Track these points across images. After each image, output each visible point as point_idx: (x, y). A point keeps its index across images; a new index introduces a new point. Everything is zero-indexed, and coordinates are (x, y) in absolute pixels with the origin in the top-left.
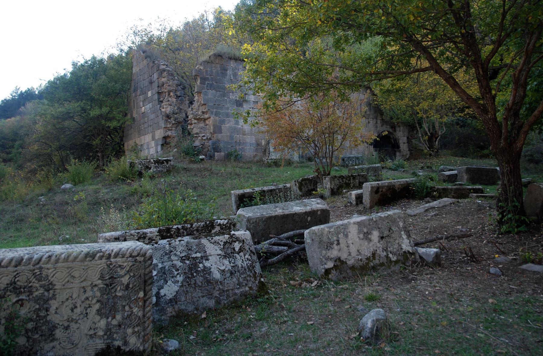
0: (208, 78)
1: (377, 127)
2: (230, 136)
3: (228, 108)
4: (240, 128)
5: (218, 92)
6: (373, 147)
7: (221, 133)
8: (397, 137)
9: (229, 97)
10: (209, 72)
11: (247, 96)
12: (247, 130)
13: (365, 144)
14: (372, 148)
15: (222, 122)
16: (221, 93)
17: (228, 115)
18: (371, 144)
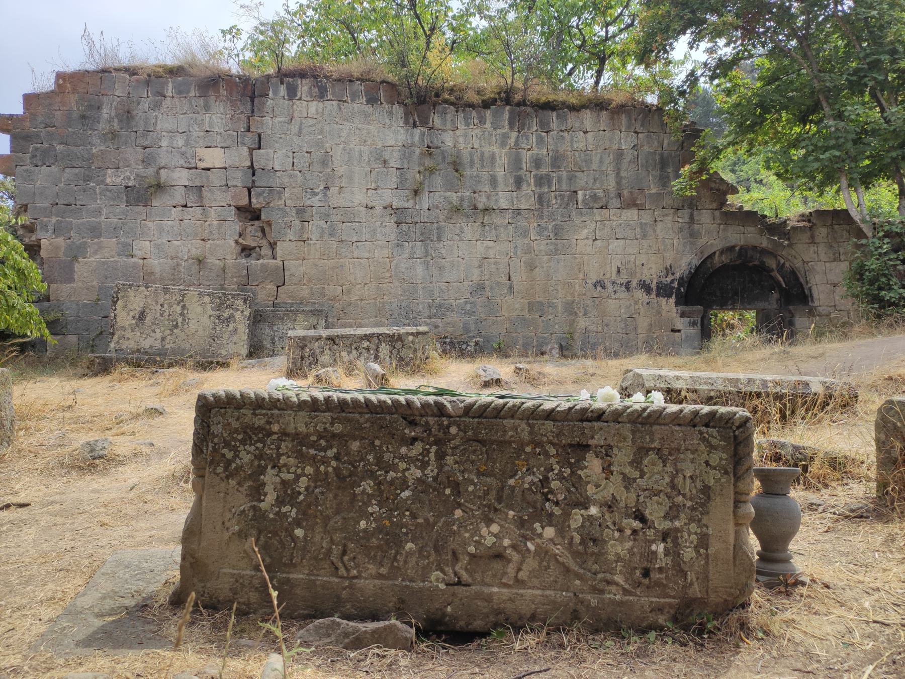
0: (37, 135)
1: (693, 235)
2: (100, 288)
3: (98, 212)
4: (135, 266)
5: (67, 170)
6: (677, 304)
7: (71, 280)
8: (798, 264)
9: (103, 182)
10: (40, 119)
11: (162, 170)
12: (157, 270)
13: (640, 294)
14: (669, 306)
15: (76, 253)
16: (77, 170)
17: (95, 231)
18: (664, 291)
